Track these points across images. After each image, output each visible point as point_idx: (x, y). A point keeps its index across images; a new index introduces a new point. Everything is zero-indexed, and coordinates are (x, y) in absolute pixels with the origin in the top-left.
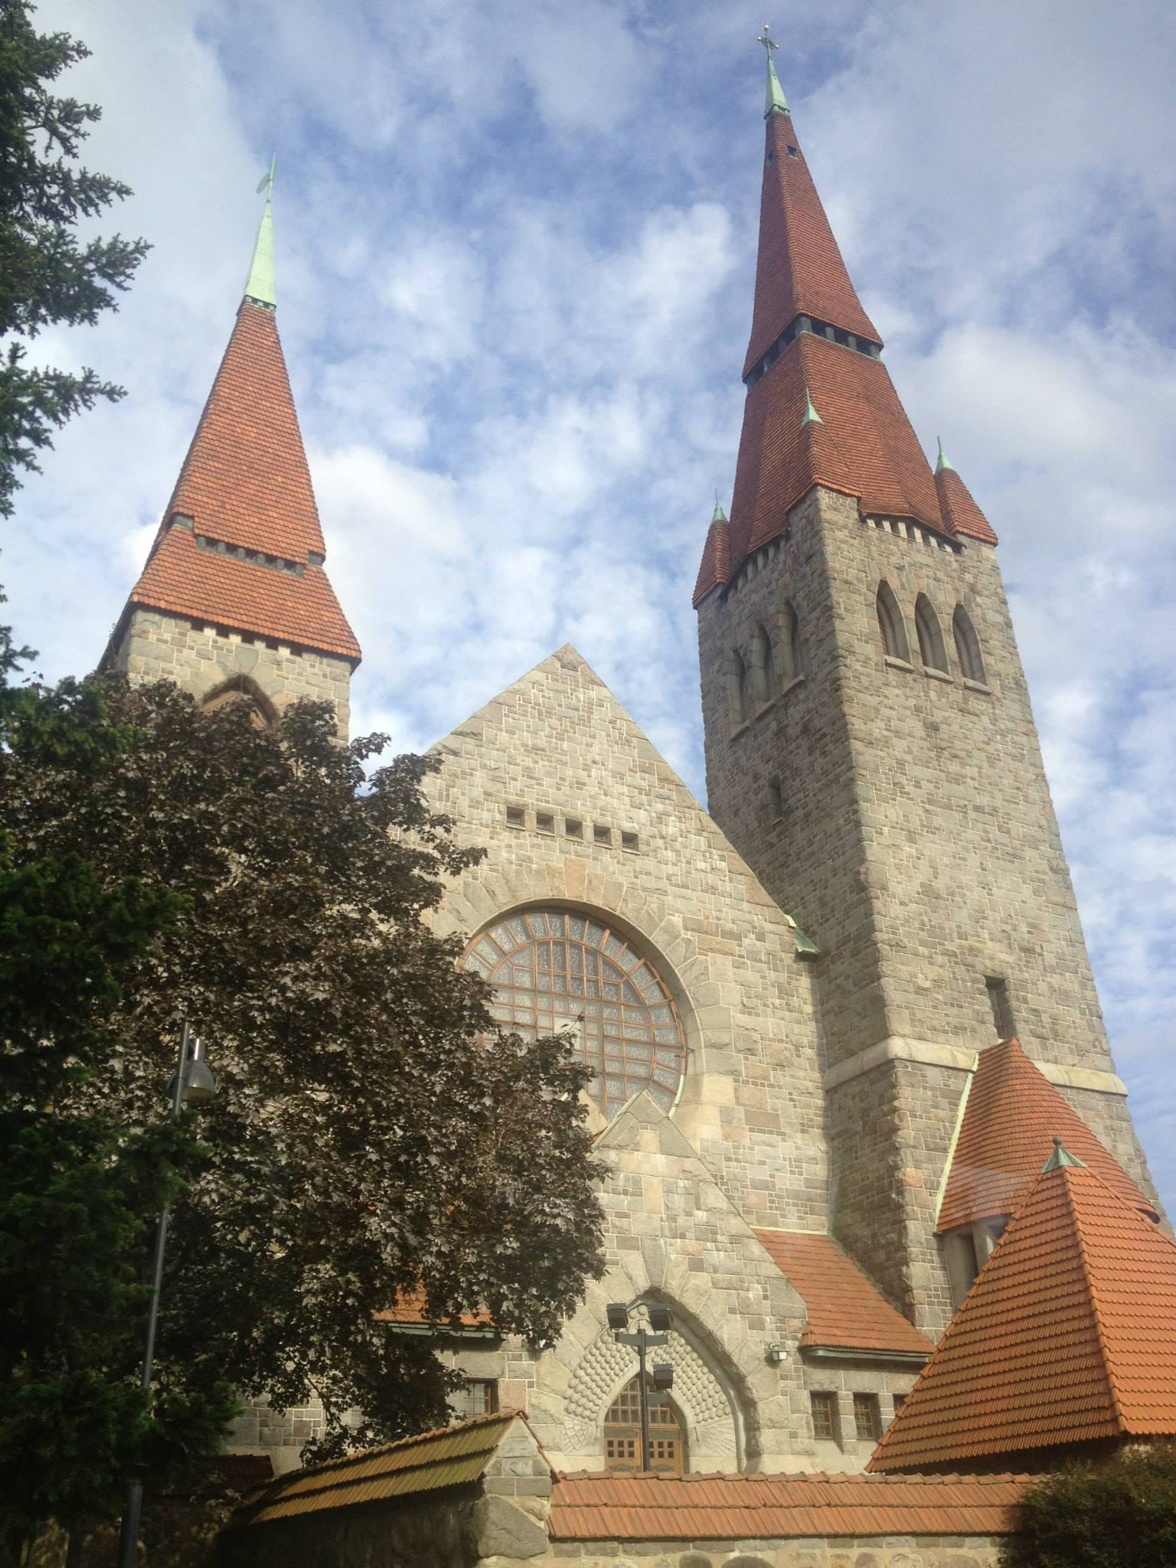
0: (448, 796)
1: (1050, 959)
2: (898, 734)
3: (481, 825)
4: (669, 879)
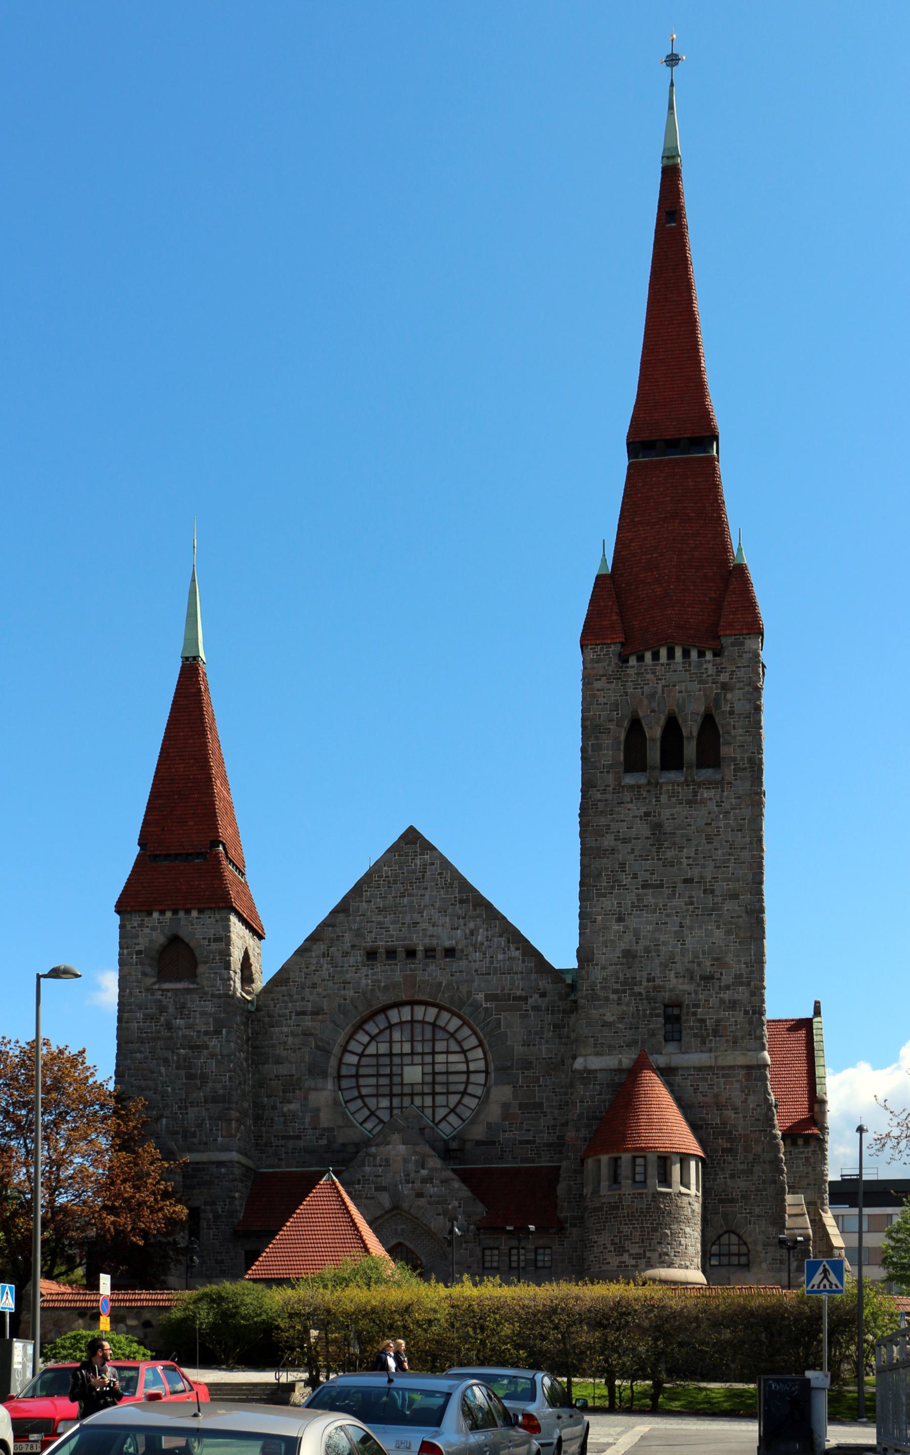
0: (328, 954)
1: (727, 979)
2: (625, 841)
3: (349, 966)
4: (476, 971)
